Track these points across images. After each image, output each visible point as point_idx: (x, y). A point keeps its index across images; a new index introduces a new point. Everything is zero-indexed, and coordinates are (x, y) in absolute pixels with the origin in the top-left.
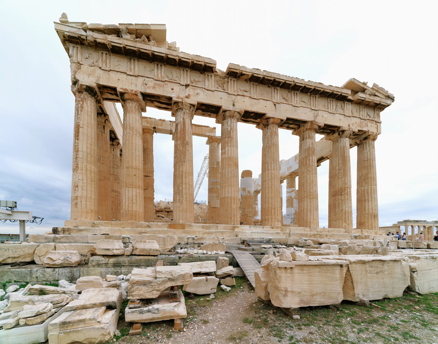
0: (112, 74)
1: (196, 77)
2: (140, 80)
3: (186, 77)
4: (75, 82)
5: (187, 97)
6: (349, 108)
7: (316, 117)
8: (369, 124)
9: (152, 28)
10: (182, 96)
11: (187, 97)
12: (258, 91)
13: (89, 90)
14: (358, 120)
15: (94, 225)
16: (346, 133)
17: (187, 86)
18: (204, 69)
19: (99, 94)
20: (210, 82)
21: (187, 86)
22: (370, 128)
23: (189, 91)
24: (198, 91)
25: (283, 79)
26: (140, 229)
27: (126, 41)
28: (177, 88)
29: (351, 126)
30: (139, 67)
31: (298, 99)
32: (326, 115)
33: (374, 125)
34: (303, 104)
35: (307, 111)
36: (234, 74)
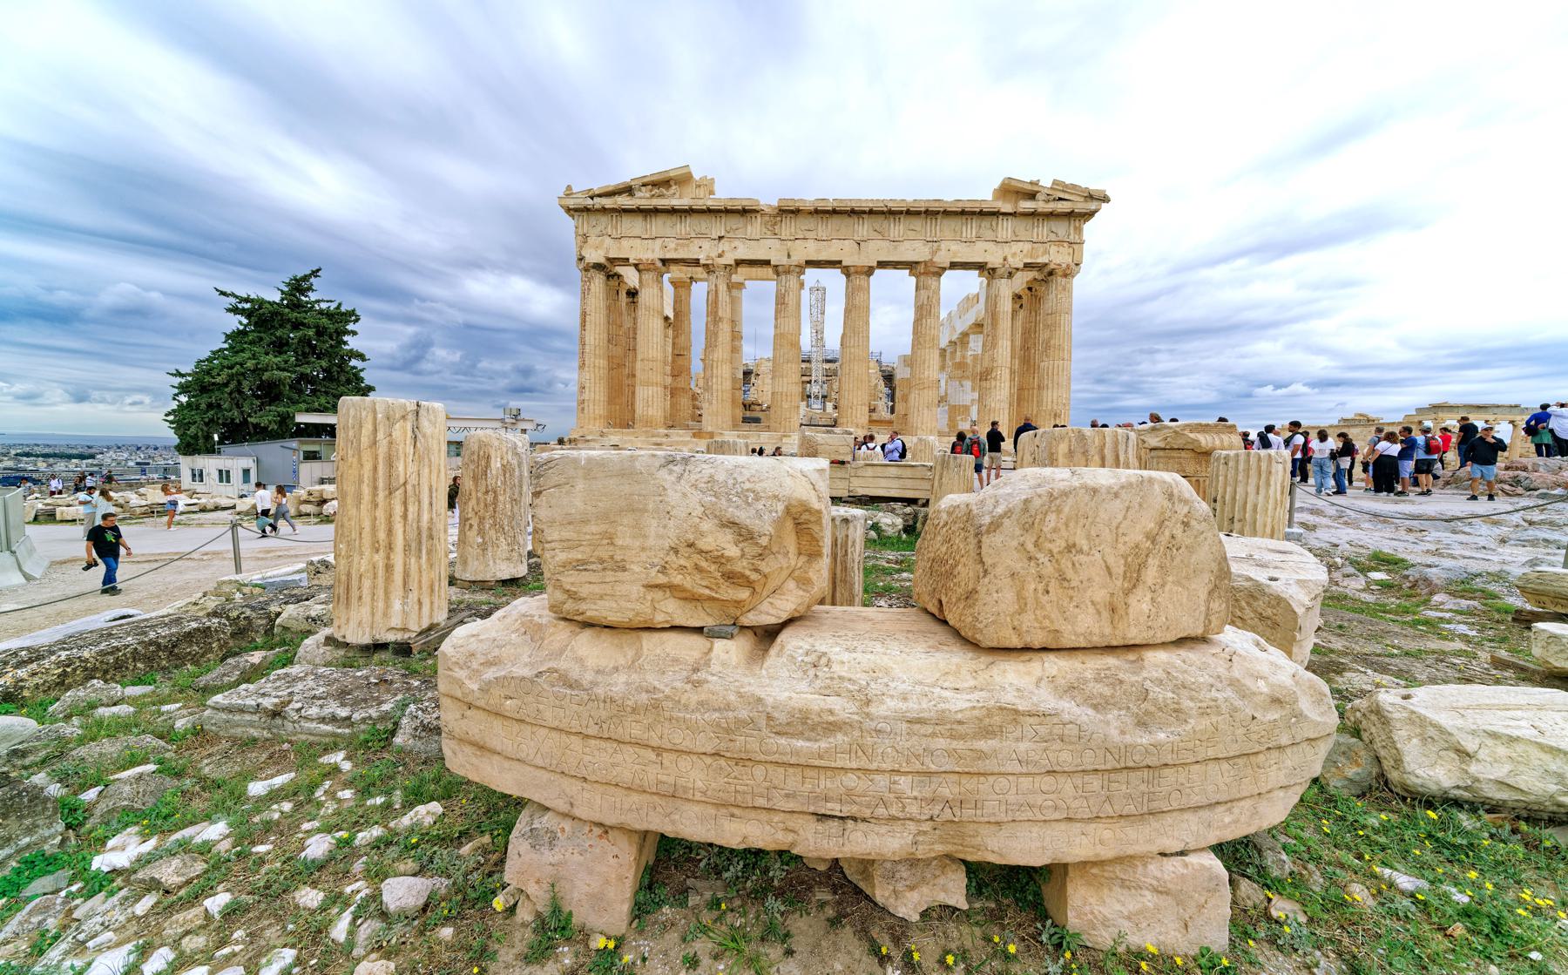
0: (624, 242)
1: (734, 222)
2: (659, 241)
3: (717, 227)
4: (581, 259)
5: (720, 256)
6: (1006, 228)
7: (934, 253)
8: (1053, 249)
9: (672, 174)
10: (714, 254)
11: (720, 256)
12: (824, 228)
13: (598, 267)
14: (1027, 246)
15: (602, 435)
16: (999, 272)
17: (721, 238)
18: (745, 212)
19: (608, 270)
20: (755, 227)
21: (721, 238)
22: (1057, 257)
23: (724, 245)
24: (736, 243)
25: (866, 206)
26: (654, 439)
27: (643, 199)
28: (706, 244)
29: (1010, 259)
30: (658, 225)
31: (897, 229)
32: (954, 247)
33: (1065, 249)
34: (911, 235)
35: (918, 244)
36: (789, 212)
